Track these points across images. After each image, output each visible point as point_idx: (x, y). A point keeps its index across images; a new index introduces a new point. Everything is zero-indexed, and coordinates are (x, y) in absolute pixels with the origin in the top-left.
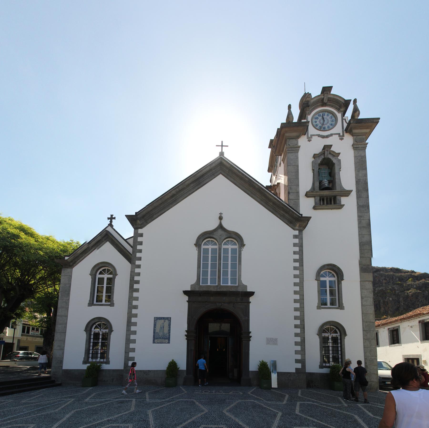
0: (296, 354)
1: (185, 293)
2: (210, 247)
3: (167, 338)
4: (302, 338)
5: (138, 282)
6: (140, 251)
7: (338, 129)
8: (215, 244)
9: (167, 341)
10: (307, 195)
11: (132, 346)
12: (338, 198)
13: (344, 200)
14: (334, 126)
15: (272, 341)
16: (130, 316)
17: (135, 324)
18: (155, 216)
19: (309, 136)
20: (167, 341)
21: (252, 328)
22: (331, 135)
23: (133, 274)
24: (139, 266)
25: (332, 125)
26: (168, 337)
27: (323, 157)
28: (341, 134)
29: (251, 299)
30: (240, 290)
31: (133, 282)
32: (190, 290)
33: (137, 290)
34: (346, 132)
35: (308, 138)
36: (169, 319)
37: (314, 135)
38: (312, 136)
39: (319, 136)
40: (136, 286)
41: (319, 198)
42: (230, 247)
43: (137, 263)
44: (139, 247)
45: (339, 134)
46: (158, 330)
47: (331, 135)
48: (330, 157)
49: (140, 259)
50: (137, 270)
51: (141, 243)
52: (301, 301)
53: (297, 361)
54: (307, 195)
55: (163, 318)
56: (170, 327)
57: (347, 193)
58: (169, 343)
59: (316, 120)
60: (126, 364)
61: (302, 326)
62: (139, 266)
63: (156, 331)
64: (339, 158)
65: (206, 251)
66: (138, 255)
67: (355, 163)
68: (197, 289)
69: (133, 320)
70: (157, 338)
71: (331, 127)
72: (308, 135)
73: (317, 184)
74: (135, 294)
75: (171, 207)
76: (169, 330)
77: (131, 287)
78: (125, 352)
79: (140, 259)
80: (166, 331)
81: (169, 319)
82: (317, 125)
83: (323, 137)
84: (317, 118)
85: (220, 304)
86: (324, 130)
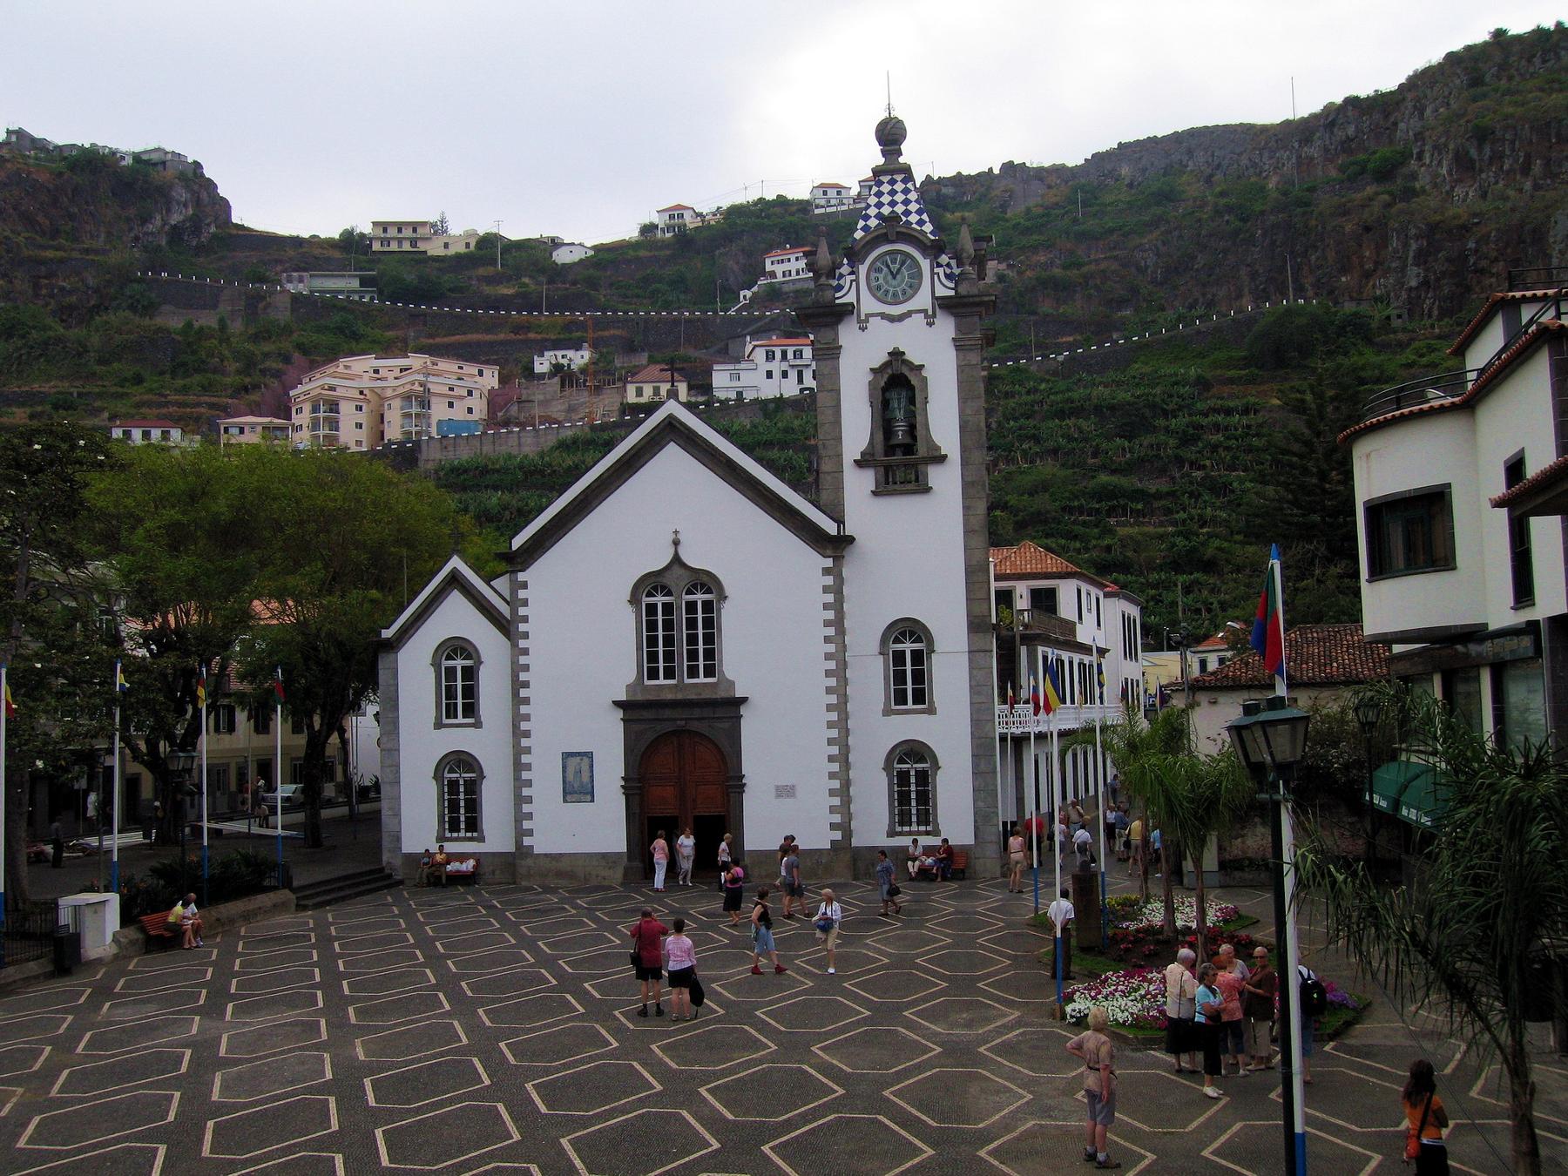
0: (831, 813)
1: (617, 704)
2: (659, 600)
3: (587, 793)
4: (843, 782)
5: (526, 685)
6: (525, 619)
7: (923, 299)
8: (669, 594)
9: (589, 798)
10: (860, 464)
11: (526, 808)
12: (921, 468)
13: (935, 475)
14: (915, 288)
15: (785, 792)
16: (519, 751)
17: (528, 767)
18: (547, 544)
19: (863, 317)
20: (589, 798)
21: (746, 768)
22: (909, 314)
23: (517, 669)
24: (526, 652)
25: (911, 287)
26: (590, 790)
27: (890, 371)
28: (930, 312)
29: (743, 710)
30: (722, 694)
31: (518, 685)
32: (624, 698)
33: (526, 701)
34: (940, 308)
35: (859, 321)
36: (589, 755)
37: (873, 315)
38: (868, 316)
39: (884, 316)
40: (523, 693)
41: (882, 469)
42: (699, 597)
43: (522, 644)
44: (522, 611)
45: (925, 311)
46: (570, 777)
47: (909, 314)
48: (905, 371)
49: (526, 635)
50: (523, 660)
51: (525, 603)
52: (841, 707)
53: (833, 826)
54: (860, 464)
55: (579, 754)
56: (592, 771)
57: (941, 459)
58: (592, 801)
59: (877, 275)
60: (519, 844)
61: (843, 759)
62: (526, 652)
63: (568, 779)
64: (924, 373)
65: (651, 609)
66: (522, 627)
67: (960, 382)
68: (639, 697)
69: (525, 759)
70: (570, 793)
71: (910, 291)
72: (859, 315)
73: (880, 436)
74: (524, 709)
75: (578, 523)
76: (592, 777)
77: (515, 694)
78: (516, 821)
79: (526, 635)
80: (586, 779)
81: (589, 755)
82: (879, 288)
83: (892, 319)
84: (879, 270)
85: (683, 722)
86: (896, 302)
